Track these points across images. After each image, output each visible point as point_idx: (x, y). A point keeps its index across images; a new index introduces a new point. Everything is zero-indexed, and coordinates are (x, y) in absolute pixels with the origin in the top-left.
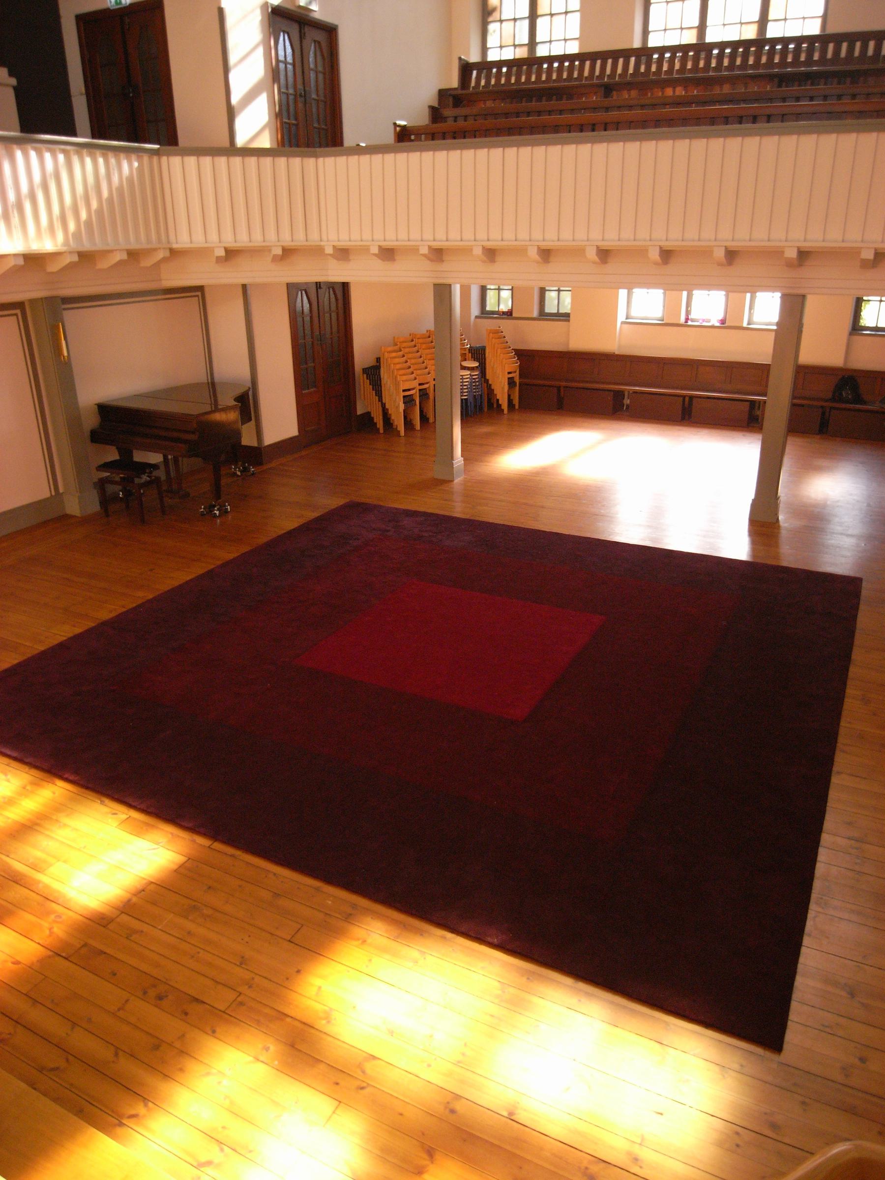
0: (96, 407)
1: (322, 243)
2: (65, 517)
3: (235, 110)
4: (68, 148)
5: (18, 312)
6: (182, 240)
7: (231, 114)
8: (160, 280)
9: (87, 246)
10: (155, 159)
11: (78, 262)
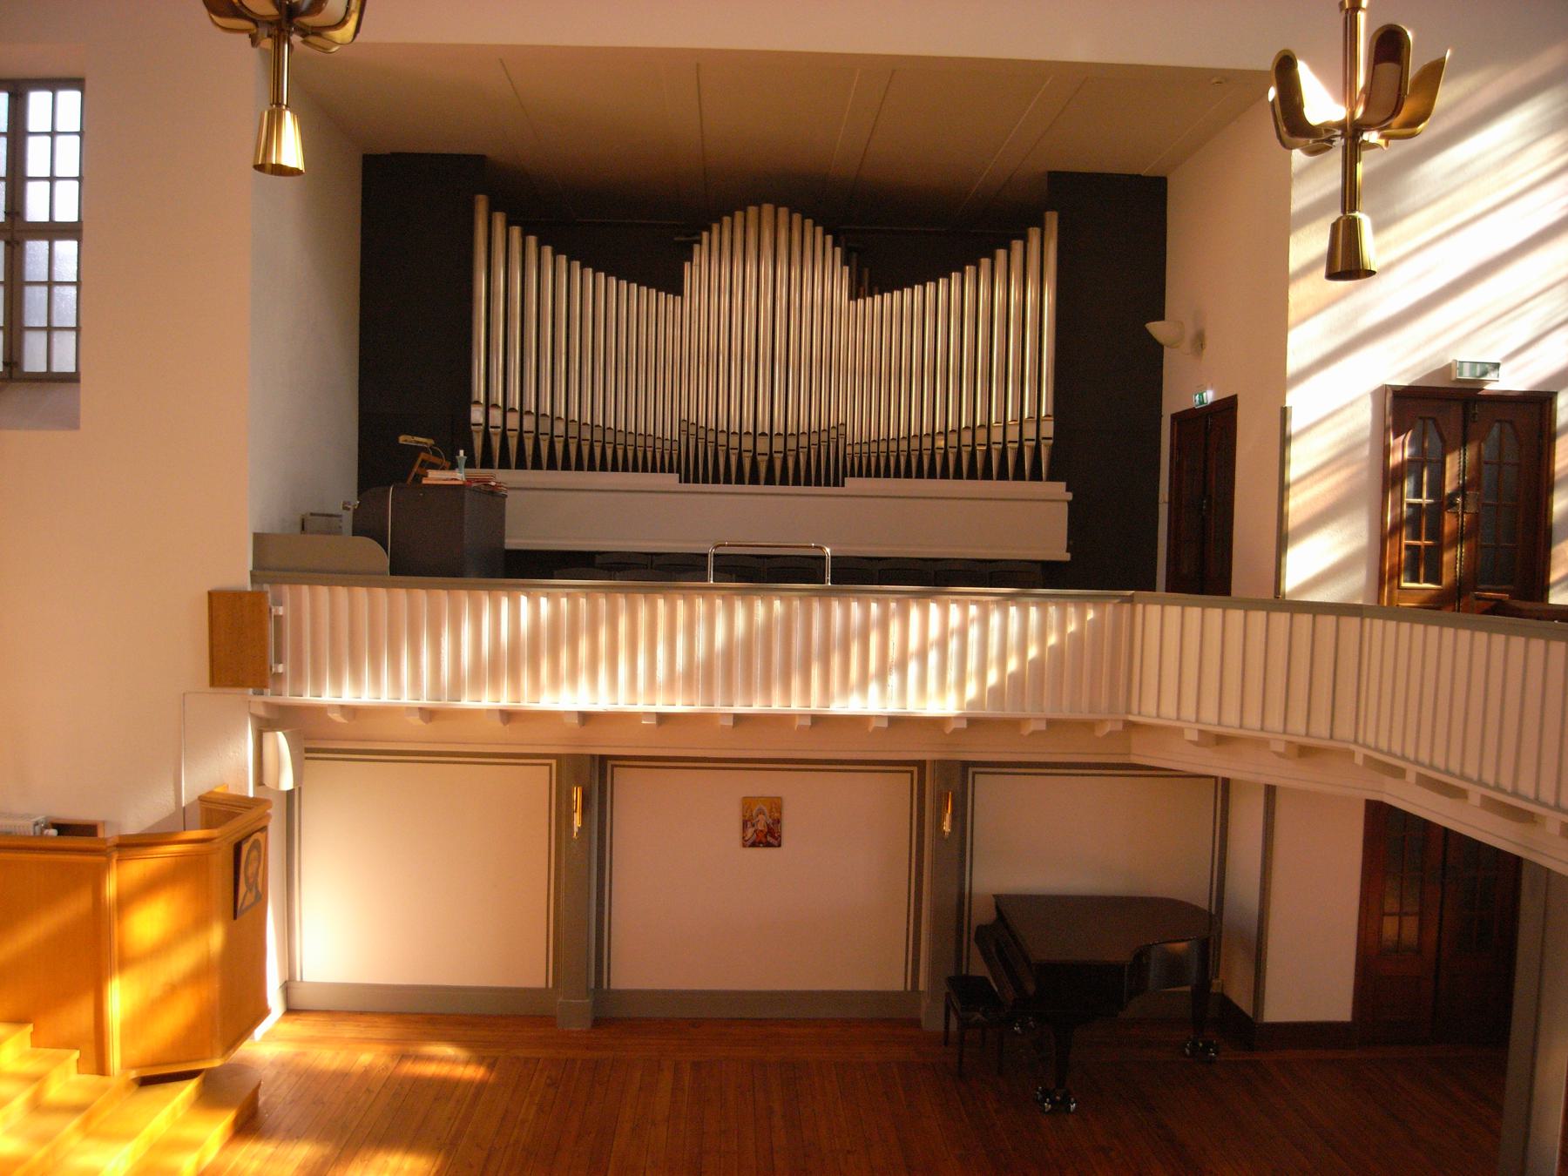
0: (993, 900)
1: (1353, 747)
2: (916, 1023)
3: (1290, 536)
5: (915, 769)
6: (1146, 712)
7: (1282, 542)
8: (1129, 754)
9: (987, 711)
10: (1127, 607)
11: (966, 729)
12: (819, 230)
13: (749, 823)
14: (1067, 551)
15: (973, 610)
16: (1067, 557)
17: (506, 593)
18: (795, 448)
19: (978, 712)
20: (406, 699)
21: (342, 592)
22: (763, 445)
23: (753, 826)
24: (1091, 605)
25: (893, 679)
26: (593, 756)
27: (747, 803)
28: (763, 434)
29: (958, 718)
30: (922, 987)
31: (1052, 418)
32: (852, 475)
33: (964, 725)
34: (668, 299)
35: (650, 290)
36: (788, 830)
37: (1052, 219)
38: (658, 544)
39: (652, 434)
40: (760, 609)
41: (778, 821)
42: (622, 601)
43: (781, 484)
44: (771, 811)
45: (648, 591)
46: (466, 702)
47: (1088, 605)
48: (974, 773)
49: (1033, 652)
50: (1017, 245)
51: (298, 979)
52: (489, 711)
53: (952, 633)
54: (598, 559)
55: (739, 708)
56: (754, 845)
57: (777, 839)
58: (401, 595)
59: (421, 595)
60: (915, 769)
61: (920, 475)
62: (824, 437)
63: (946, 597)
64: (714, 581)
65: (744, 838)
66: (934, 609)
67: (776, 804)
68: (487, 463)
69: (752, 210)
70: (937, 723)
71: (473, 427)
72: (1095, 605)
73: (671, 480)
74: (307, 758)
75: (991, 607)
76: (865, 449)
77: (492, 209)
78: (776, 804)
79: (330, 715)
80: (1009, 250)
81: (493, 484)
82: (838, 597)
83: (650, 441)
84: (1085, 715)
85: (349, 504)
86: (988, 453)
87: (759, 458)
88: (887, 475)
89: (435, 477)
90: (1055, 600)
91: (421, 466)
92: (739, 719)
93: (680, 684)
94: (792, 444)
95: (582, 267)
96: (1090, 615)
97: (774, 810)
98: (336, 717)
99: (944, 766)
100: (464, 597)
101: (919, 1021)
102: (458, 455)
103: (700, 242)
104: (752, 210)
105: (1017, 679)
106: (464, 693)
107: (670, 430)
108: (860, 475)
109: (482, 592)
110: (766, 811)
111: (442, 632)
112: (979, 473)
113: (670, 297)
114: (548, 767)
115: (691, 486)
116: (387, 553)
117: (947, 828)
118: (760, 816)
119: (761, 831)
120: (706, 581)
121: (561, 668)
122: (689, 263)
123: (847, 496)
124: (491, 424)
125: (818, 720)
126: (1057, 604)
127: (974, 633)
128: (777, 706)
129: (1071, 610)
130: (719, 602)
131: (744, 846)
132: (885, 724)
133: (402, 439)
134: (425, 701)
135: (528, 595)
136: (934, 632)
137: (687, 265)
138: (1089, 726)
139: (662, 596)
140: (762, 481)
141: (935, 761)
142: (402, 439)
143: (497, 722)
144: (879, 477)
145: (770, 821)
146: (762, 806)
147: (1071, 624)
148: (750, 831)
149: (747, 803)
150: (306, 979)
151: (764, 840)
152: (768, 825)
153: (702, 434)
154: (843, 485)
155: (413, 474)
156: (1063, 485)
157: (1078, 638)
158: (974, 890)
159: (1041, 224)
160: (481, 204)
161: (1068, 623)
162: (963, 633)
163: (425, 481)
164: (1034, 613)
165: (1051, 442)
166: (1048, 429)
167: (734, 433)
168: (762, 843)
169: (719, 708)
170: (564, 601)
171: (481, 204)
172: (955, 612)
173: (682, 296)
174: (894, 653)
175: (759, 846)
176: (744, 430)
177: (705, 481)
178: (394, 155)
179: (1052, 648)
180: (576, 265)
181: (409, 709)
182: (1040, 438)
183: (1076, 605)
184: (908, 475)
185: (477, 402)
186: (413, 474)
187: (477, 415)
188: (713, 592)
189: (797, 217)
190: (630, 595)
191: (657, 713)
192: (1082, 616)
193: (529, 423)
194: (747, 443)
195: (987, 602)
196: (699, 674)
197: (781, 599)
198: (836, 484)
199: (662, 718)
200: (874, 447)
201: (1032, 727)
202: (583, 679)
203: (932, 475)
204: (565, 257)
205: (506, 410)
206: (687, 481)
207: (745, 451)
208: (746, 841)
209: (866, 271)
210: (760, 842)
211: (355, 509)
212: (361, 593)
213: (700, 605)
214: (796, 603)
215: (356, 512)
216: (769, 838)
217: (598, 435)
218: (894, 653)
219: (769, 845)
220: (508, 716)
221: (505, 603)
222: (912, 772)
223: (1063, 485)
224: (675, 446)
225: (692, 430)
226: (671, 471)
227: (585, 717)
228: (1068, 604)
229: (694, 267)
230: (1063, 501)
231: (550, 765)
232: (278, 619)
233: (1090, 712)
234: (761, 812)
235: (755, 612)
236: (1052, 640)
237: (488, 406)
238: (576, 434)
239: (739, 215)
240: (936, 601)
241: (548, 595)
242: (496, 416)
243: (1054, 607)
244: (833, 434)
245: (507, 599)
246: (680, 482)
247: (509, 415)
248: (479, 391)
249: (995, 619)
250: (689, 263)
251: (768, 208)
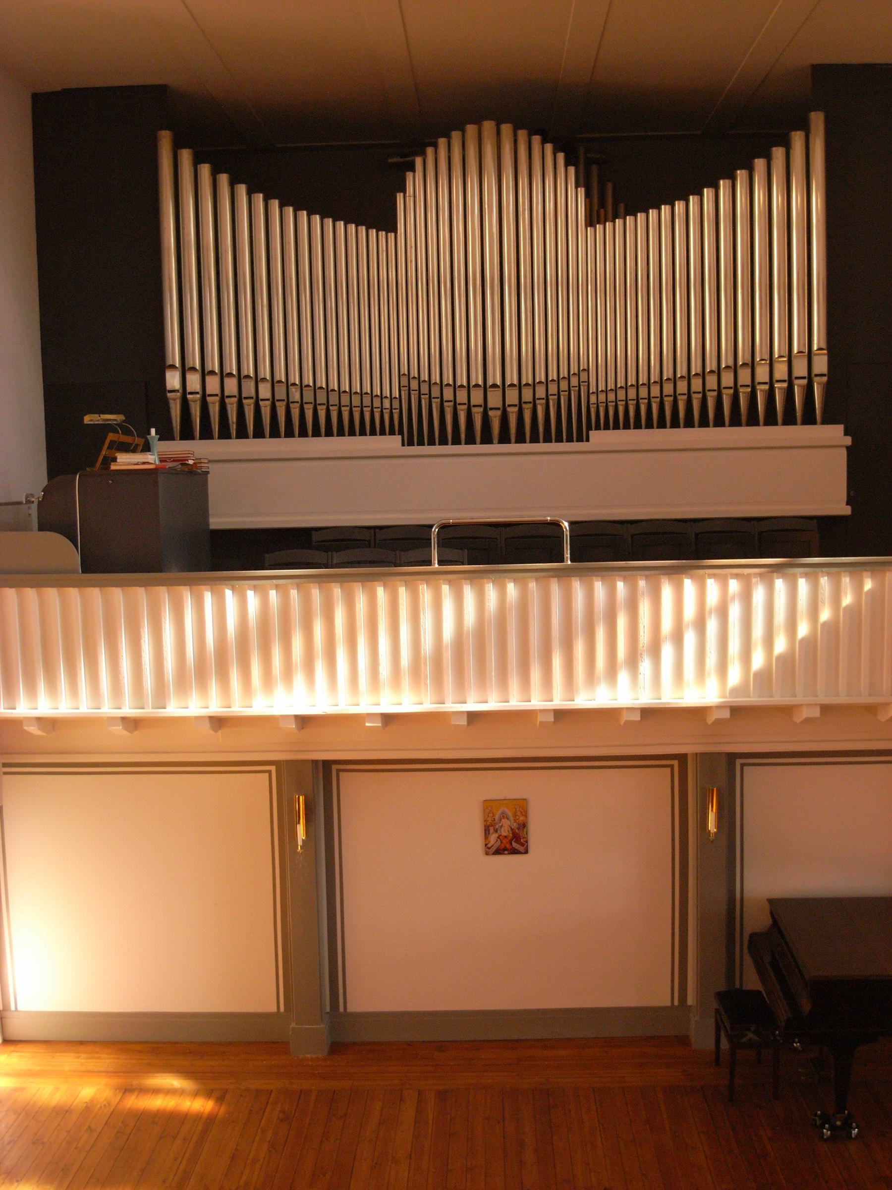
2: (683, 1040)
4: (746, 571)
5: (675, 763)
9: (753, 698)
12: (549, 147)
13: (491, 829)
14: (847, 504)
15: (734, 586)
16: (847, 510)
17: (208, 587)
18: (531, 400)
19: (742, 700)
20: (107, 709)
21: (31, 594)
22: (494, 400)
23: (496, 831)
24: (869, 574)
25: (645, 666)
26: (315, 762)
27: (489, 806)
28: (494, 386)
29: (719, 707)
30: (691, 1000)
31: (825, 352)
32: (598, 428)
33: (726, 714)
34: (380, 237)
35: (359, 228)
36: (535, 835)
37: (817, 120)
38: (379, 516)
39: (369, 391)
40: (491, 592)
41: (524, 825)
42: (337, 591)
43: (517, 442)
44: (515, 815)
45: (365, 579)
46: (173, 709)
47: (865, 574)
48: (743, 765)
49: (803, 630)
50: (778, 153)
51: (13, 1008)
52: (197, 718)
53: (710, 612)
54: (315, 537)
55: (473, 706)
56: (498, 852)
57: (522, 845)
58: (95, 593)
59: (117, 594)
60: (675, 763)
61: (675, 424)
62: (564, 385)
63: (701, 572)
65: (486, 845)
66: (688, 584)
67: (521, 807)
68: (187, 434)
69: (471, 129)
70: (697, 713)
71: (169, 395)
72: (873, 574)
73: (392, 443)
74: (5, 773)
75: (754, 580)
76: (611, 397)
77: (177, 146)
78: (521, 807)
79: (25, 728)
80: (768, 157)
81: (191, 462)
82: (579, 576)
83: (367, 401)
84: (865, 699)
85: (32, 495)
86: (753, 396)
87: (491, 413)
88: (638, 426)
89: (125, 461)
90: (824, 570)
91: (110, 447)
92: (473, 717)
93: (406, 681)
94: (527, 395)
95: (282, 206)
96: (868, 585)
97: (518, 813)
98: (33, 729)
99: (706, 758)
100: (163, 592)
101: (687, 1038)
102: (149, 433)
103: (412, 169)
104: (471, 129)
105: (787, 661)
106: (170, 696)
107: (391, 388)
108: (607, 427)
109: (182, 587)
110: (510, 815)
111: (142, 634)
112: (744, 418)
113: (382, 234)
114: (267, 775)
115: (416, 450)
116: (77, 550)
117: (712, 826)
118: (503, 820)
119: (506, 837)
120: (430, 565)
121: (273, 668)
122: (402, 194)
123: (592, 452)
124: (189, 390)
125: (560, 715)
126: (828, 574)
127: (735, 611)
128: (515, 703)
129: (846, 580)
130: (445, 588)
131: (487, 854)
132: (637, 717)
133: (88, 419)
134: (128, 710)
135: (233, 589)
136: (690, 612)
137: (400, 197)
138: (871, 709)
139: (382, 583)
140: (496, 439)
141: (696, 754)
142: (88, 419)
143: (206, 729)
144: (629, 428)
145: (515, 825)
146: (506, 810)
147: (846, 593)
148: (493, 838)
149: (489, 806)
150: (20, 1008)
151: (508, 846)
152: (512, 829)
153: (425, 389)
154: (588, 440)
155: (101, 458)
156: (840, 428)
157: (854, 612)
158: (745, 896)
159: (805, 126)
160: (165, 141)
161: (843, 594)
162: (723, 612)
163: (113, 467)
164: (803, 585)
165: (825, 379)
166: (821, 364)
167: (462, 386)
168: (507, 850)
169: (451, 706)
170: (273, 594)
171: (165, 141)
172: (712, 587)
173: (394, 230)
174: (644, 636)
175: (503, 854)
176: (473, 383)
177: (431, 443)
178: (65, 91)
179: (824, 624)
180: (275, 204)
181: (112, 720)
182: (813, 375)
183: (851, 574)
184: (662, 425)
185: (173, 367)
186: (101, 458)
187: (173, 380)
188: (437, 577)
189: (522, 134)
190: (346, 584)
191: (382, 714)
192: (860, 586)
193: (231, 386)
194: (477, 397)
195: (749, 575)
196: (427, 669)
197: (515, 581)
198: (580, 439)
199: (388, 719)
200: (621, 395)
201: (806, 713)
202: (299, 678)
203: (689, 424)
204: (261, 195)
205: (204, 374)
206: (411, 443)
207: (474, 406)
208: (489, 848)
209: (610, 186)
210: (505, 849)
211: (39, 502)
212: (52, 593)
213: (425, 592)
214: (533, 585)
215: (40, 504)
216: (514, 844)
217: (308, 396)
218: (644, 636)
219: (514, 852)
220: (218, 722)
221: (208, 598)
222: (672, 767)
223: (840, 428)
224: (396, 404)
225: (414, 385)
226: (392, 433)
227: (304, 721)
228: (843, 574)
229: (407, 199)
230: (842, 446)
231: (269, 772)
233: (870, 695)
234: (504, 816)
235: (487, 597)
236: (825, 615)
237: (185, 370)
238: (284, 397)
239: (456, 135)
240: (692, 577)
241: (255, 588)
242: (194, 381)
243: (826, 578)
244: (574, 381)
245: (210, 593)
246: (403, 445)
247: (209, 379)
248: (174, 354)
249: (759, 594)
250: (402, 194)
251: (489, 126)
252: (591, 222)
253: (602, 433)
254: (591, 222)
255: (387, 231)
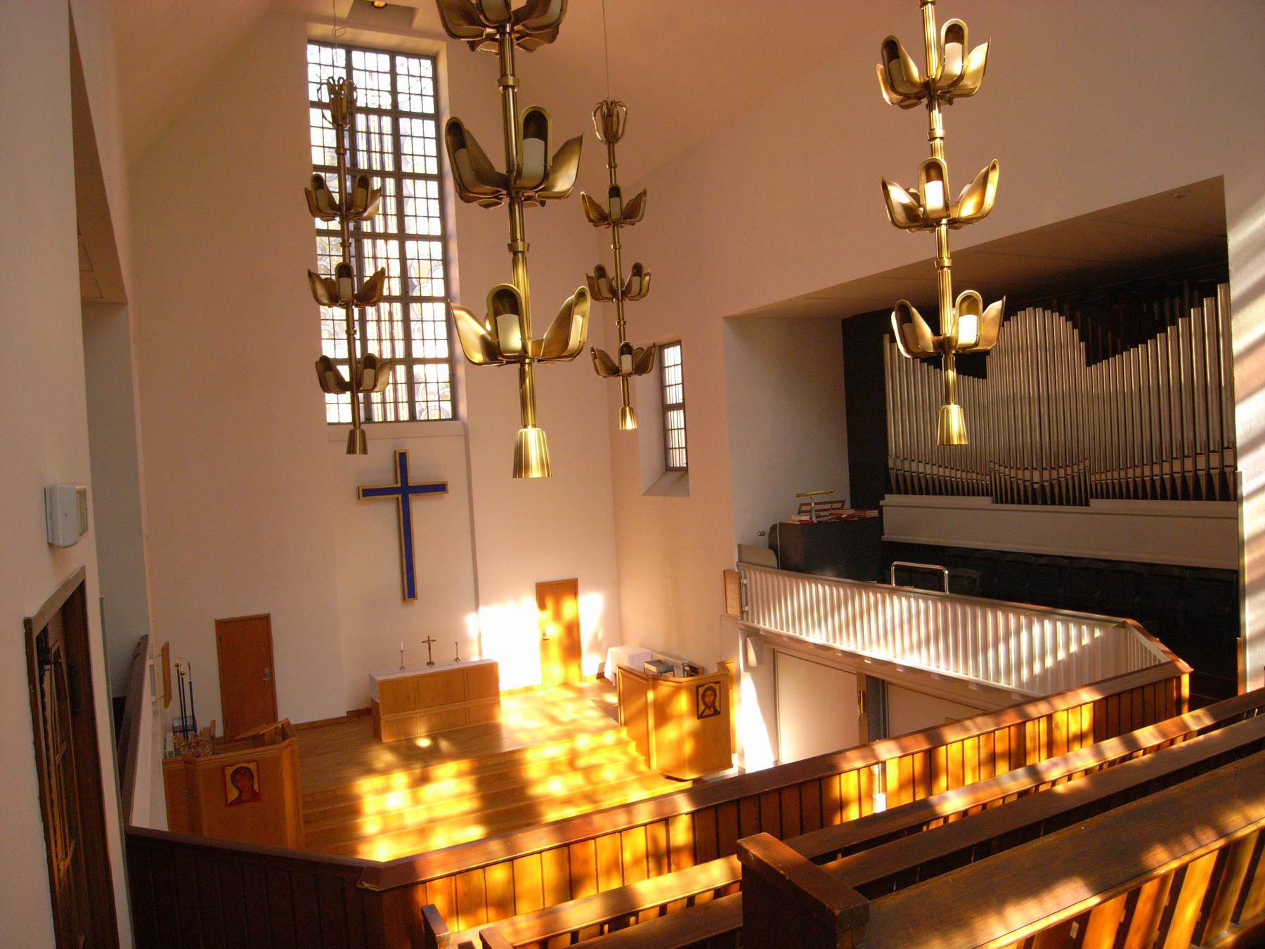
15: (1023, 620)
32: (1097, 497)
64: (896, 584)
72: (1101, 627)
73: (986, 501)
95: (934, 368)
96: (1098, 633)
115: (1000, 506)
192: (1092, 633)
198: (1087, 504)
206: (997, 503)
226: (987, 495)
232: (745, 585)
252: (1089, 364)
253: (1099, 501)
254: (1089, 364)
255: (983, 379)
